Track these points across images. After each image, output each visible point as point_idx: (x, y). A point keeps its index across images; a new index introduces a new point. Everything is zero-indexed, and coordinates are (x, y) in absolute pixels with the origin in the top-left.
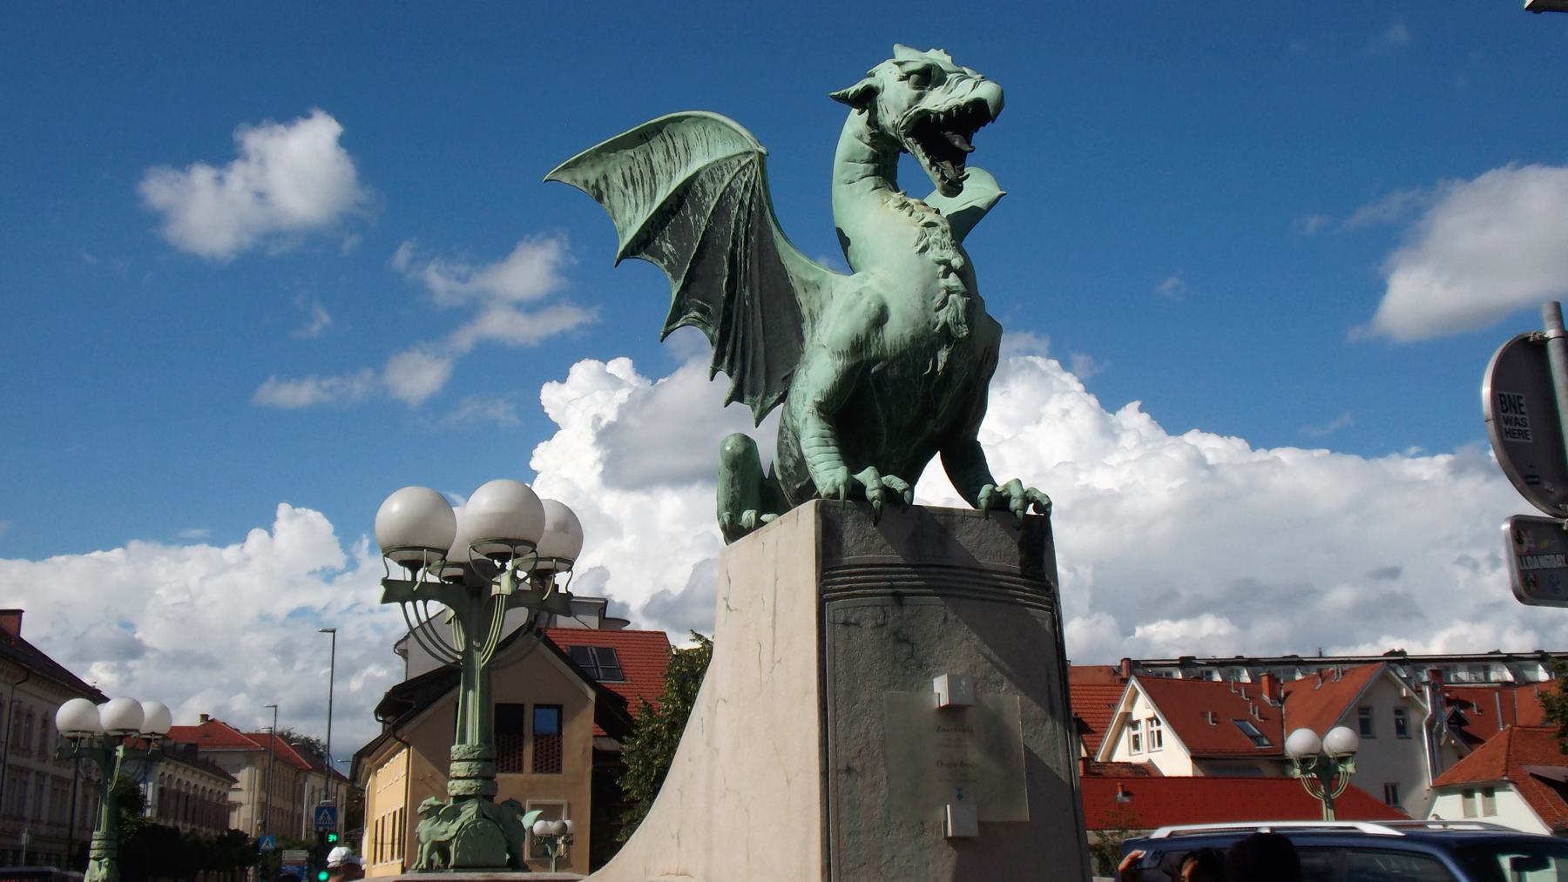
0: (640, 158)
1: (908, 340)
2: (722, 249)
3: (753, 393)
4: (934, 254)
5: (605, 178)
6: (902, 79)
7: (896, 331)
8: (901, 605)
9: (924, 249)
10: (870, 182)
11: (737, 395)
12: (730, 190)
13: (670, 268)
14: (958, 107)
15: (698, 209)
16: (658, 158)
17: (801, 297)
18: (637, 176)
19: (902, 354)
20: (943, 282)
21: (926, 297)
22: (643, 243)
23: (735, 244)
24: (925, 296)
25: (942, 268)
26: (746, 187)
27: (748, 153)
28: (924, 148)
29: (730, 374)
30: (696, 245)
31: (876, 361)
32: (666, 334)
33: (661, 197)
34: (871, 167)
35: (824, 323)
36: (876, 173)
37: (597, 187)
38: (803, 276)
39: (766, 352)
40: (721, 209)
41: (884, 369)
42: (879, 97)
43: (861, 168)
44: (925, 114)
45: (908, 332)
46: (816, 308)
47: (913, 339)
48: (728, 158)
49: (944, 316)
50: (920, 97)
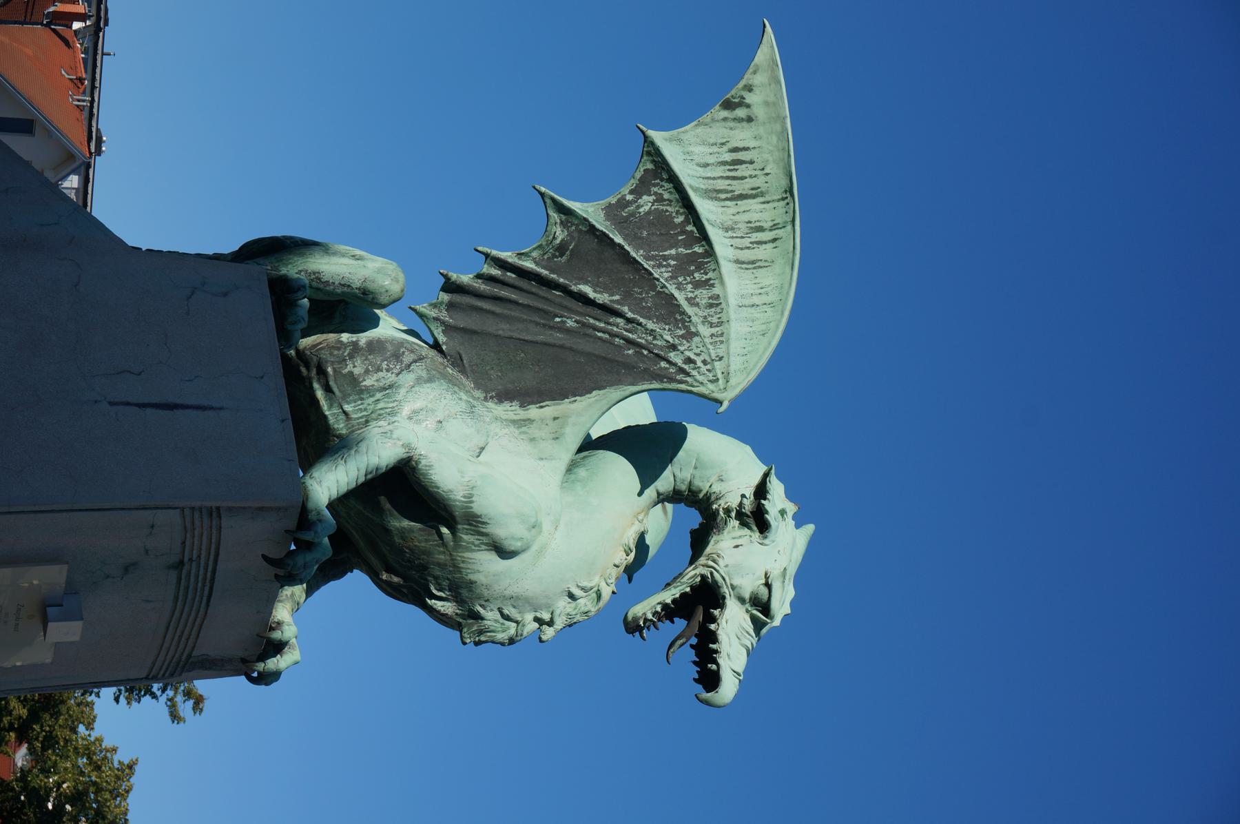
1: (472, 577)
2: (627, 297)
3: (451, 306)
4: (563, 607)
5: (750, 119)
7: (484, 567)
8: (170, 567)
9: (572, 596)
11: (450, 287)
12: (690, 335)
13: (623, 204)
15: (684, 266)
18: (743, 171)
19: (457, 569)
20: (529, 617)
21: (515, 600)
22: (661, 169)
23: (629, 321)
24: (518, 598)
25: (546, 616)
26: (689, 361)
27: (727, 375)
28: (683, 595)
33: (704, 207)
37: (742, 104)
40: (670, 311)
41: (444, 545)
44: (719, 602)
46: (534, 431)
47: (472, 582)
48: (728, 340)
49: (490, 616)
50: (742, 600)
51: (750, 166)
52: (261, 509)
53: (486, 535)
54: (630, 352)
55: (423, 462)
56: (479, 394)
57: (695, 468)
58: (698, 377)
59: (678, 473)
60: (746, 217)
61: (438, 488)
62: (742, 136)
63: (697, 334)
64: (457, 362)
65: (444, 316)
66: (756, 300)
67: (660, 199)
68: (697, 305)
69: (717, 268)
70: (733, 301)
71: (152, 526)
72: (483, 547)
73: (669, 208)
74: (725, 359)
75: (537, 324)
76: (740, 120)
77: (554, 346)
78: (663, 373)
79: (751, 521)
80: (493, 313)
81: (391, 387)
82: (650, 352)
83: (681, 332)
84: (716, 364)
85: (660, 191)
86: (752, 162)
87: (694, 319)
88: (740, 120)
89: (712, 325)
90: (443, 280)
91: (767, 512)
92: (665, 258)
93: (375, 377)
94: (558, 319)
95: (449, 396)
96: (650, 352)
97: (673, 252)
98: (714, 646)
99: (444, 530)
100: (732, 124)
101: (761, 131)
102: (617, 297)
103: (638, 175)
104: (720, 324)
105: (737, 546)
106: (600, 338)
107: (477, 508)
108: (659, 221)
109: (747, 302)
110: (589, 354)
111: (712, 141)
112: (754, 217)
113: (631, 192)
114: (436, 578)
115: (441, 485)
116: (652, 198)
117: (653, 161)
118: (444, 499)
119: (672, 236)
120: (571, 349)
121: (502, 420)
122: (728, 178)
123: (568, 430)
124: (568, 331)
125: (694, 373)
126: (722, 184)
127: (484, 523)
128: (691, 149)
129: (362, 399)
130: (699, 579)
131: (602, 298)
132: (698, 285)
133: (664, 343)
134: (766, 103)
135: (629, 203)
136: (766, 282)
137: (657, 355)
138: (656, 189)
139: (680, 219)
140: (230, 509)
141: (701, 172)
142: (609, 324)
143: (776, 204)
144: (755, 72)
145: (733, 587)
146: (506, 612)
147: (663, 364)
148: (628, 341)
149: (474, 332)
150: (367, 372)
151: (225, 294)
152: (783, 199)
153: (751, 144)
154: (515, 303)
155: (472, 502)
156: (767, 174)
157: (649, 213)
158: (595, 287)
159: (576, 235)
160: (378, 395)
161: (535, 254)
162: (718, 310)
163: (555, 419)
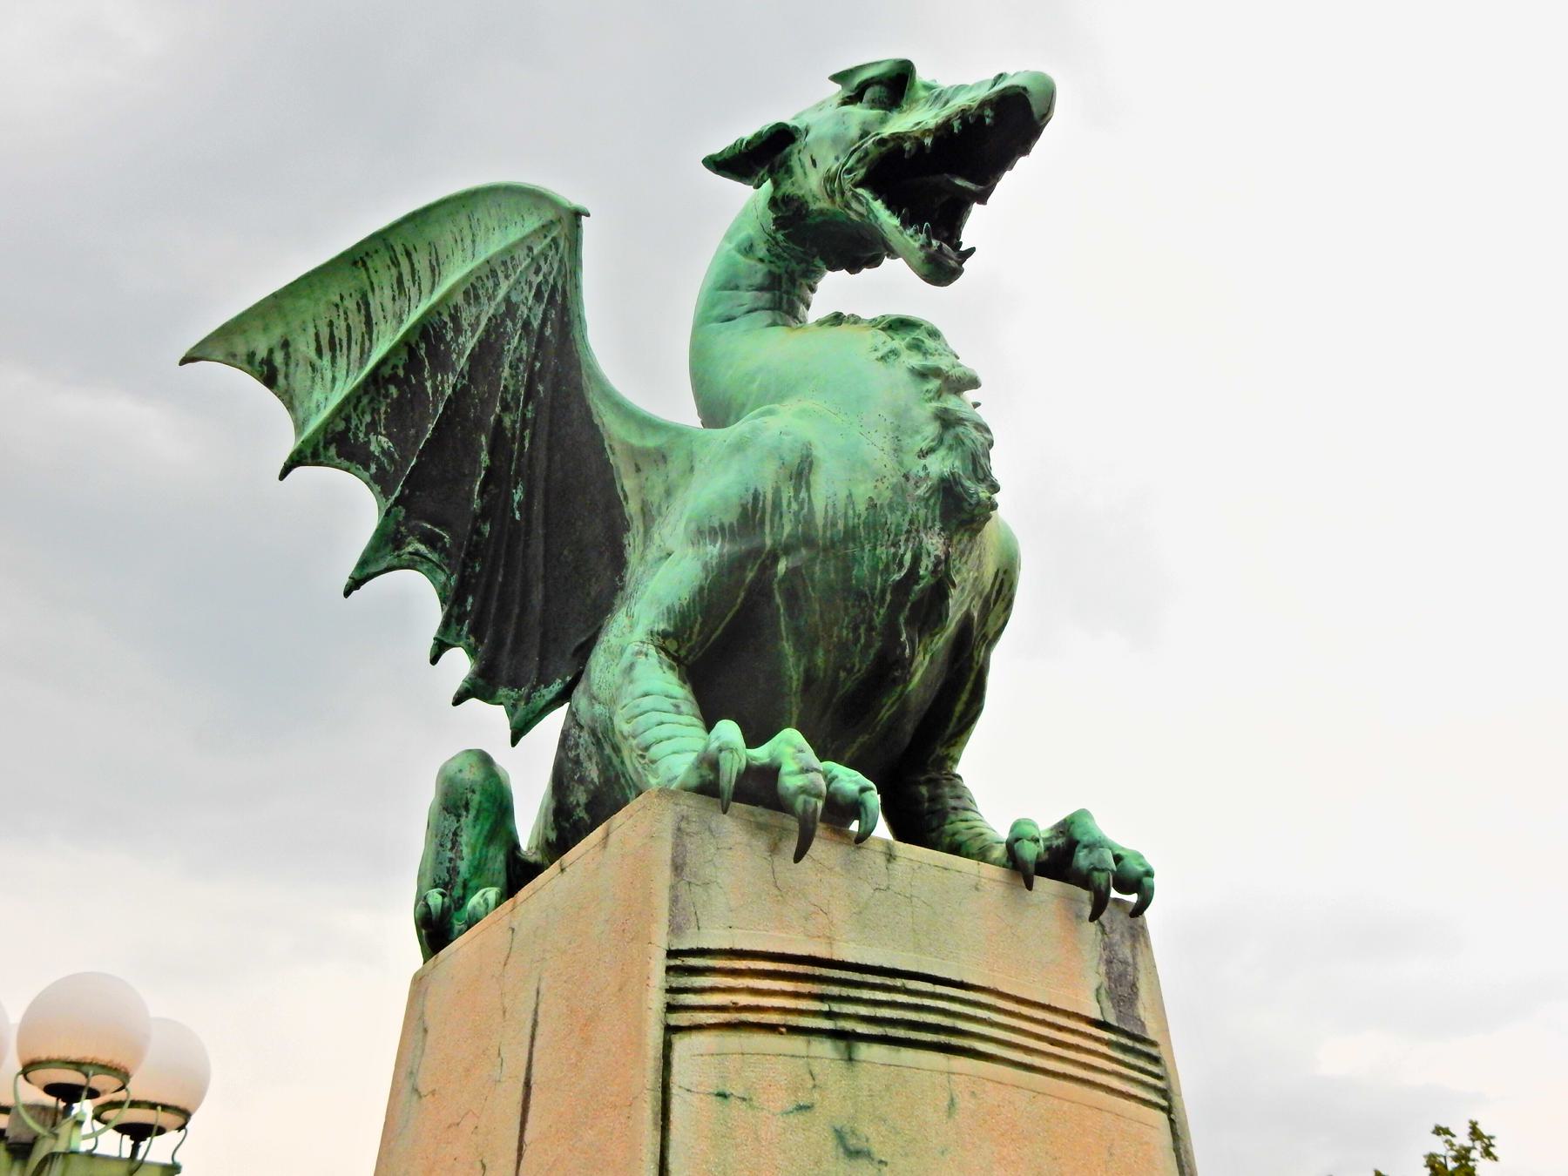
0: (350, 304)
1: (861, 507)
5: (286, 345)
6: (848, 101)
10: (766, 316)
11: (479, 687)
12: (510, 307)
14: (963, 114)
15: (441, 363)
16: (382, 299)
17: (628, 483)
18: (341, 333)
19: (850, 535)
20: (935, 404)
21: (899, 431)
23: (506, 408)
26: (538, 296)
28: (888, 208)
29: (472, 652)
30: (431, 427)
31: (788, 549)
32: (355, 584)
34: (767, 296)
35: (672, 519)
36: (775, 306)
37: (268, 362)
38: (636, 441)
39: (547, 600)
40: (488, 350)
42: (799, 144)
43: (748, 297)
45: (863, 491)
46: (655, 497)
48: (509, 250)
50: (883, 121)
51: (336, 323)
52: (678, 868)
53: (777, 492)
54: (541, 388)
55: (662, 626)
56: (617, 602)
57: (737, 288)
58: (556, 266)
59: (745, 308)
60: (388, 304)
61: (701, 589)
62: (304, 347)
63: (507, 299)
64: (584, 652)
65: (524, 691)
66: (468, 242)
67: (372, 427)
68: (478, 318)
69: (434, 311)
70: (466, 270)
71: (723, 1095)
72: (803, 494)
73: (383, 409)
74: (528, 242)
75: (527, 546)
76: (287, 356)
77: (546, 507)
78: (557, 326)
79: (779, 157)
80: (521, 616)
81: (593, 732)
82: (535, 358)
83: (509, 323)
85: (363, 428)
86: (331, 324)
87: (491, 311)
88: (287, 356)
89: (497, 285)
90: (473, 700)
91: (758, 135)
92: (435, 388)
93: (587, 764)
94: (518, 516)
95: (611, 636)
96: (535, 358)
97: (429, 384)
98: (956, 124)
99: (782, 567)
100: (292, 366)
101: (296, 324)
102: (483, 439)
103: (346, 464)
104: (494, 273)
105: (814, 163)
106: (531, 443)
107: (731, 517)
108: (401, 418)
109: (469, 253)
110: (549, 449)
111: (309, 383)
112: (388, 292)
113: (367, 468)
114: (874, 569)
115: (697, 583)
116: (373, 438)
117: (326, 448)
118: (720, 574)
119: (414, 394)
120: (547, 479)
121: (645, 547)
123: (651, 442)
124: (529, 494)
125: (551, 281)
126: (356, 350)
127: (756, 497)
128: (313, 405)
129: (617, 777)
130: (860, 191)
131: (485, 458)
132: (458, 330)
133: (524, 342)
134: (266, 329)
135: (380, 467)
136: (449, 238)
137: (538, 346)
138: (361, 435)
139: (393, 390)
140: (675, 929)
141: (339, 384)
142: (514, 434)
143: (372, 271)
144: (234, 356)
145: (864, 134)
146: (924, 445)
147: (548, 332)
148: (530, 394)
149: (544, 636)
150: (582, 780)
151: (425, 1031)
152: (364, 264)
153: (312, 331)
154: (504, 584)
155: (722, 527)
156: (342, 298)
157: (389, 436)
158: (474, 475)
159: (413, 523)
160: (608, 750)
161: (443, 578)
162: (479, 285)
163: (638, 470)
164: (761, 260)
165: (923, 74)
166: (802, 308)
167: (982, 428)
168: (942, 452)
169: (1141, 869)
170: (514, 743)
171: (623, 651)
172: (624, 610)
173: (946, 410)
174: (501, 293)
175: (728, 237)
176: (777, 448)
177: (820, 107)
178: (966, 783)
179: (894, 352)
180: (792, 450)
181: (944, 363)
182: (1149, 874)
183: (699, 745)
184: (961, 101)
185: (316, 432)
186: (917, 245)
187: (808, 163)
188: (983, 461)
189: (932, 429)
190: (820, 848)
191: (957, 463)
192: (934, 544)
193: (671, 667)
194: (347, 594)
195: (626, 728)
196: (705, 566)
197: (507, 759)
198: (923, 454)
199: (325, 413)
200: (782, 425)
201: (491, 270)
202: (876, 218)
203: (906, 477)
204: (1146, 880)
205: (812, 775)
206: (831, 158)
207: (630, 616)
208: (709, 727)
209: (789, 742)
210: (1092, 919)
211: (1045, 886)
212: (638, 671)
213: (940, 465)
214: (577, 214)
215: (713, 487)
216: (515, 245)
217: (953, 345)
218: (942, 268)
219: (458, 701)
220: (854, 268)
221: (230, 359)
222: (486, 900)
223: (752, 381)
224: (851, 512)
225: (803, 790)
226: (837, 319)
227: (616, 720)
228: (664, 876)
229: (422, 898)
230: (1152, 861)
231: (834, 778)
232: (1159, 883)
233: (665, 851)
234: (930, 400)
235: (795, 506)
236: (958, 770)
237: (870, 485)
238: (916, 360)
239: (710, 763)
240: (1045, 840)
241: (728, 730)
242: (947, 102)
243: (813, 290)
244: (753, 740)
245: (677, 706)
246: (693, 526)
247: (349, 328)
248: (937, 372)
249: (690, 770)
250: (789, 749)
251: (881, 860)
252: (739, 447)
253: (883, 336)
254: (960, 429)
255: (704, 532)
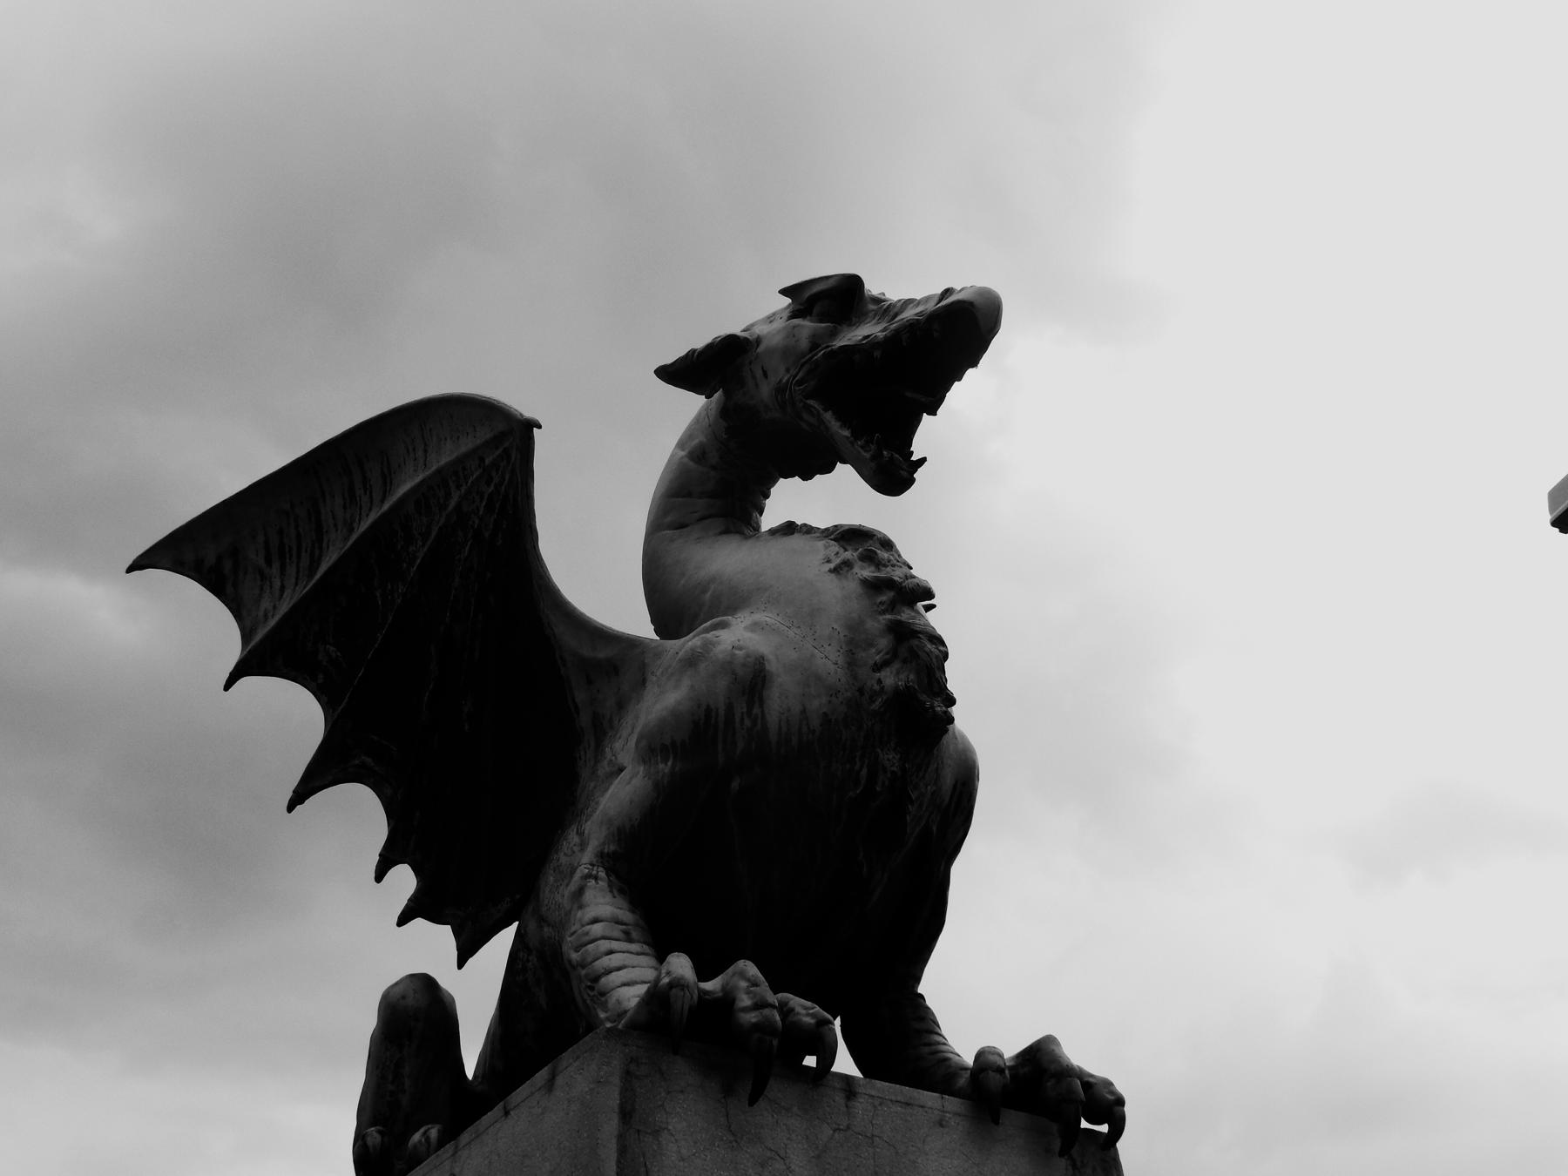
1: (816, 723)
17: (580, 696)
20: (888, 617)
21: (854, 642)
28: (839, 418)
32: (300, 796)
35: (625, 733)
38: (586, 652)
45: (817, 704)
48: (460, 461)
50: (833, 334)
52: (626, 1114)
53: (730, 708)
55: (612, 848)
57: (689, 495)
66: (420, 453)
70: (418, 480)
72: (756, 710)
84: (487, 462)
87: (443, 520)
89: (448, 495)
90: (419, 924)
122: (299, 557)
123: (603, 654)
128: (261, 613)
141: (288, 592)
145: (814, 346)
164: (714, 468)
165: (873, 287)
166: (756, 514)
167: (939, 641)
168: (896, 665)
169: (1111, 1097)
170: (461, 965)
171: (573, 871)
172: (574, 827)
173: (899, 623)
174: (453, 503)
175: (681, 444)
176: (730, 663)
177: (770, 319)
178: (928, 1003)
179: (847, 564)
180: (744, 665)
181: (897, 574)
182: (1120, 1102)
183: (650, 974)
184: (909, 314)
185: (262, 642)
186: (868, 455)
187: (759, 373)
188: (938, 674)
189: (884, 643)
190: (775, 1089)
191: (912, 677)
192: (890, 758)
193: (621, 891)
194: (290, 808)
195: (575, 956)
196: (656, 785)
197: (449, 978)
198: (878, 667)
199: (272, 623)
200: (738, 635)
201: (442, 479)
202: (827, 428)
203: (861, 691)
204: (1117, 1108)
205: (767, 1011)
206: (782, 370)
207: (580, 834)
208: (661, 958)
209: (742, 975)
210: (1061, 1154)
211: (1013, 1120)
212: (589, 895)
213: (889, 678)
214: (530, 426)
215: (662, 701)
216: (467, 456)
217: (906, 556)
218: (894, 473)
219: (403, 920)
220: (806, 476)
221: (178, 567)
222: (428, 1139)
223: (704, 591)
224: (805, 729)
225: (756, 1027)
226: (789, 528)
227: (565, 948)
228: (610, 1126)
229: (360, 1137)
230: (1121, 1087)
231: (792, 1010)
232: (1129, 1110)
233: (613, 1098)
234: (884, 612)
235: (747, 722)
236: (921, 990)
237: (824, 700)
238: (867, 572)
239: (658, 998)
240: (1011, 1068)
241: (681, 965)
242: (896, 315)
243: (767, 496)
244: (704, 973)
245: (627, 933)
246: (644, 743)
247: (298, 536)
248: (889, 584)
249: (639, 1005)
250: (745, 978)
251: (839, 1098)
252: (692, 661)
253: (835, 547)
254: (915, 642)
255: (653, 748)
